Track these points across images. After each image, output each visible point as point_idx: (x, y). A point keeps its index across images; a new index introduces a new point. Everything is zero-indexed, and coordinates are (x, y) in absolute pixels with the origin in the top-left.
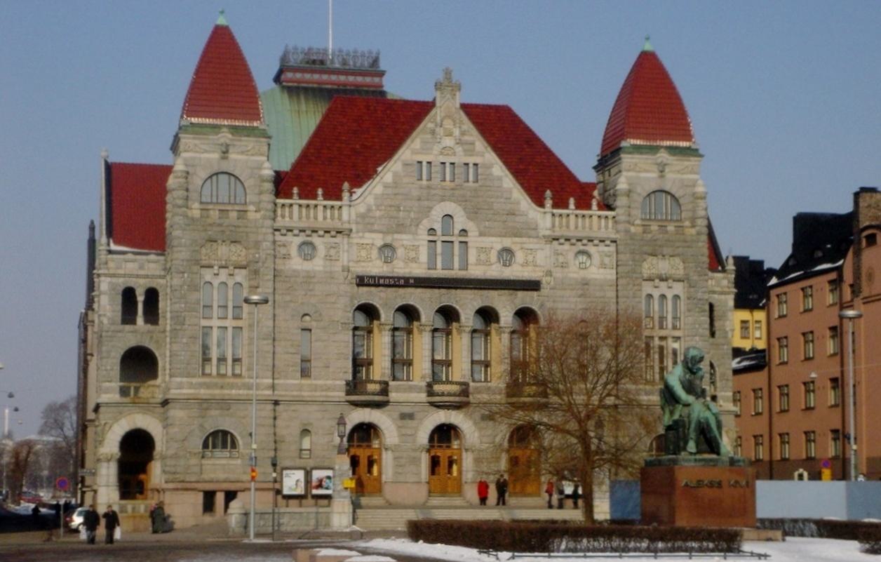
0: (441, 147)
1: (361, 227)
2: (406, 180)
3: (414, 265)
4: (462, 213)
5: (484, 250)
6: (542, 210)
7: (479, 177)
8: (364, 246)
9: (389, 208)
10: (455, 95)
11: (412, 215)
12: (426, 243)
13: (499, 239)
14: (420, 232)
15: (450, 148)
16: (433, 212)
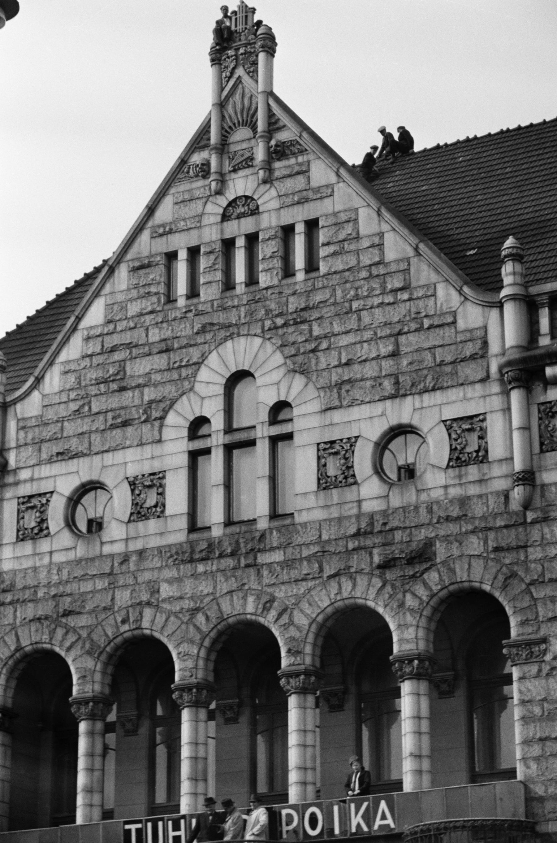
0: (225, 203)
1: (28, 451)
2: (133, 309)
3: (152, 525)
4: (278, 359)
5: (337, 447)
6: (489, 297)
7: (323, 252)
8: (35, 501)
9: (93, 390)
10: (255, 63)
11: (149, 394)
12: (184, 460)
13: (378, 408)
14: (168, 434)
15: (247, 197)
16: (204, 374)
